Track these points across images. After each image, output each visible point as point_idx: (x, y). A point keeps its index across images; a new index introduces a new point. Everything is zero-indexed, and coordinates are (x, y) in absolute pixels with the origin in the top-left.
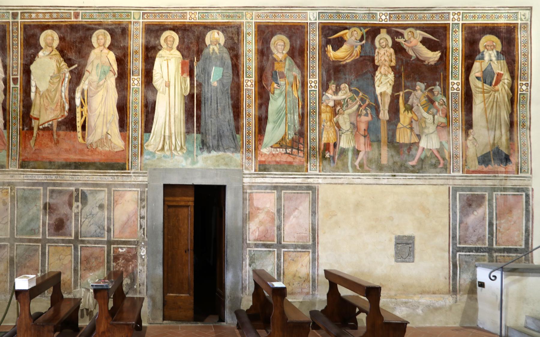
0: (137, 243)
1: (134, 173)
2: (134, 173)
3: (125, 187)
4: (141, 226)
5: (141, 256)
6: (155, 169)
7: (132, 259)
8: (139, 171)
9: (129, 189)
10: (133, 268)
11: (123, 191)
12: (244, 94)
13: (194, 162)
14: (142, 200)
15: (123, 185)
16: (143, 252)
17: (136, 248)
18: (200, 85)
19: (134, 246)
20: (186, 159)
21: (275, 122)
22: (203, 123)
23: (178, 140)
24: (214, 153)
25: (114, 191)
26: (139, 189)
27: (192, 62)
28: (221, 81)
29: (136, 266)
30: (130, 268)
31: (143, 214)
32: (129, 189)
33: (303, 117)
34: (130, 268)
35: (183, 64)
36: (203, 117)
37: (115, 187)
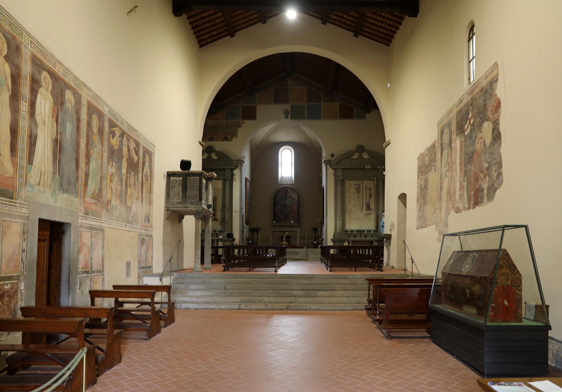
0: (18, 278)
1: (19, 203)
2: (19, 203)
3: (11, 218)
4: (22, 260)
5: (21, 291)
6: (34, 202)
7: (14, 295)
8: (23, 202)
9: (15, 220)
10: (15, 304)
11: (10, 221)
12: (81, 150)
13: (56, 201)
14: (24, 232)
15: (9, 215)
16: (22, 287)
17: (17, 283)
18: (61, 133)
19: (16, 281)
20: (52, 197)
21: (92, 179)
22: (61, 168)
23: (48, 178)
24: (66, 196)
25: (3, 220)
26: (22, 221)
27: (58, 110)
28: (71, 134)
29: (17, 302)
30: (13, 305)
31: (25, 247)
32: (15, 220)
33: (101, 178)
34: (13, 305)
35: (53, 109)
36: (61, 162)
37: (4, 217)
